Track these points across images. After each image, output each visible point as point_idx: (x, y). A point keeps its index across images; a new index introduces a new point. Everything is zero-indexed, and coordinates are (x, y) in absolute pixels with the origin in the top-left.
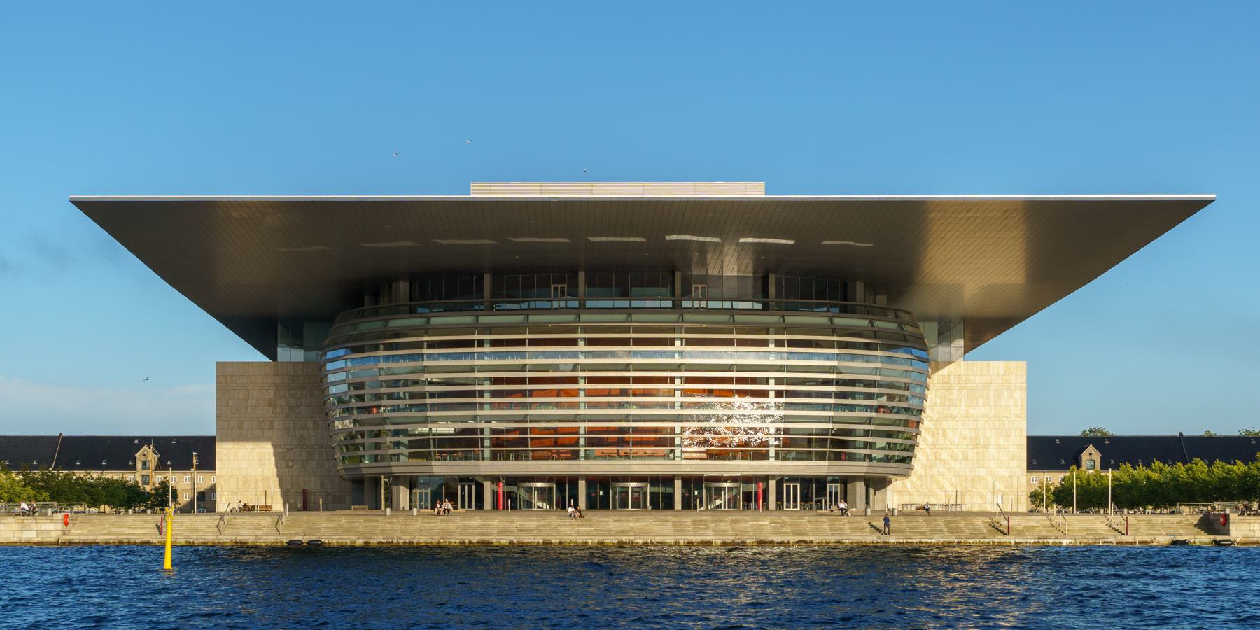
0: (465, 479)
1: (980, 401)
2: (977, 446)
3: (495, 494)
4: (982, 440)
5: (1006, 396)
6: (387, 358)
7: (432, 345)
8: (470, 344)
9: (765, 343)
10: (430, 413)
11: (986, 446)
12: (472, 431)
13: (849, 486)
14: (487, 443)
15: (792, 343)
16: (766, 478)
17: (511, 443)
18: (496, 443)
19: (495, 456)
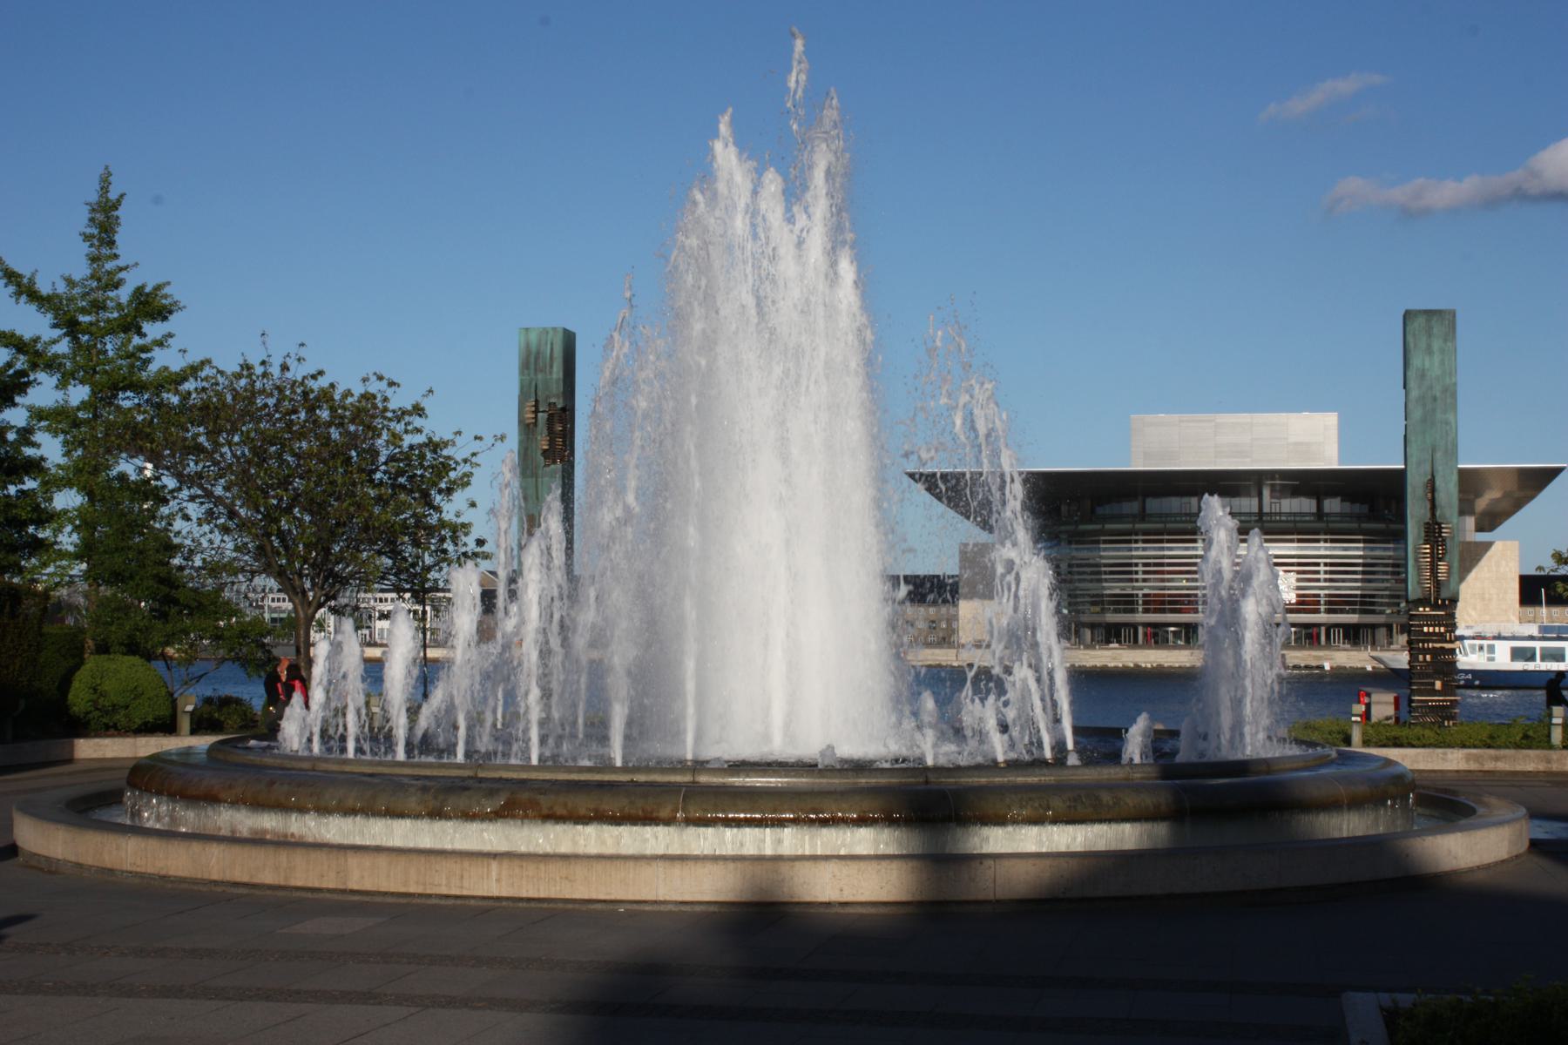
0: (1126, 625)
1: (1486, 568)
2: (1483, 599)
3: (1145, 634)
4: (1487, 596)
5: (1504, 563)
6: (1076, 549)
7: (1105, 542)
8: (1129, 542)
9: (1318, 541)
10: (1105, 584)
11: (1490, 600)
12: (1132, 595)
13: (1376, 631)
14: (1140, 602)
15: (1333, 541)
16: (1318, 625)
17: (1155, 602)
18: (1145, 603)
19: (1146, 611)
